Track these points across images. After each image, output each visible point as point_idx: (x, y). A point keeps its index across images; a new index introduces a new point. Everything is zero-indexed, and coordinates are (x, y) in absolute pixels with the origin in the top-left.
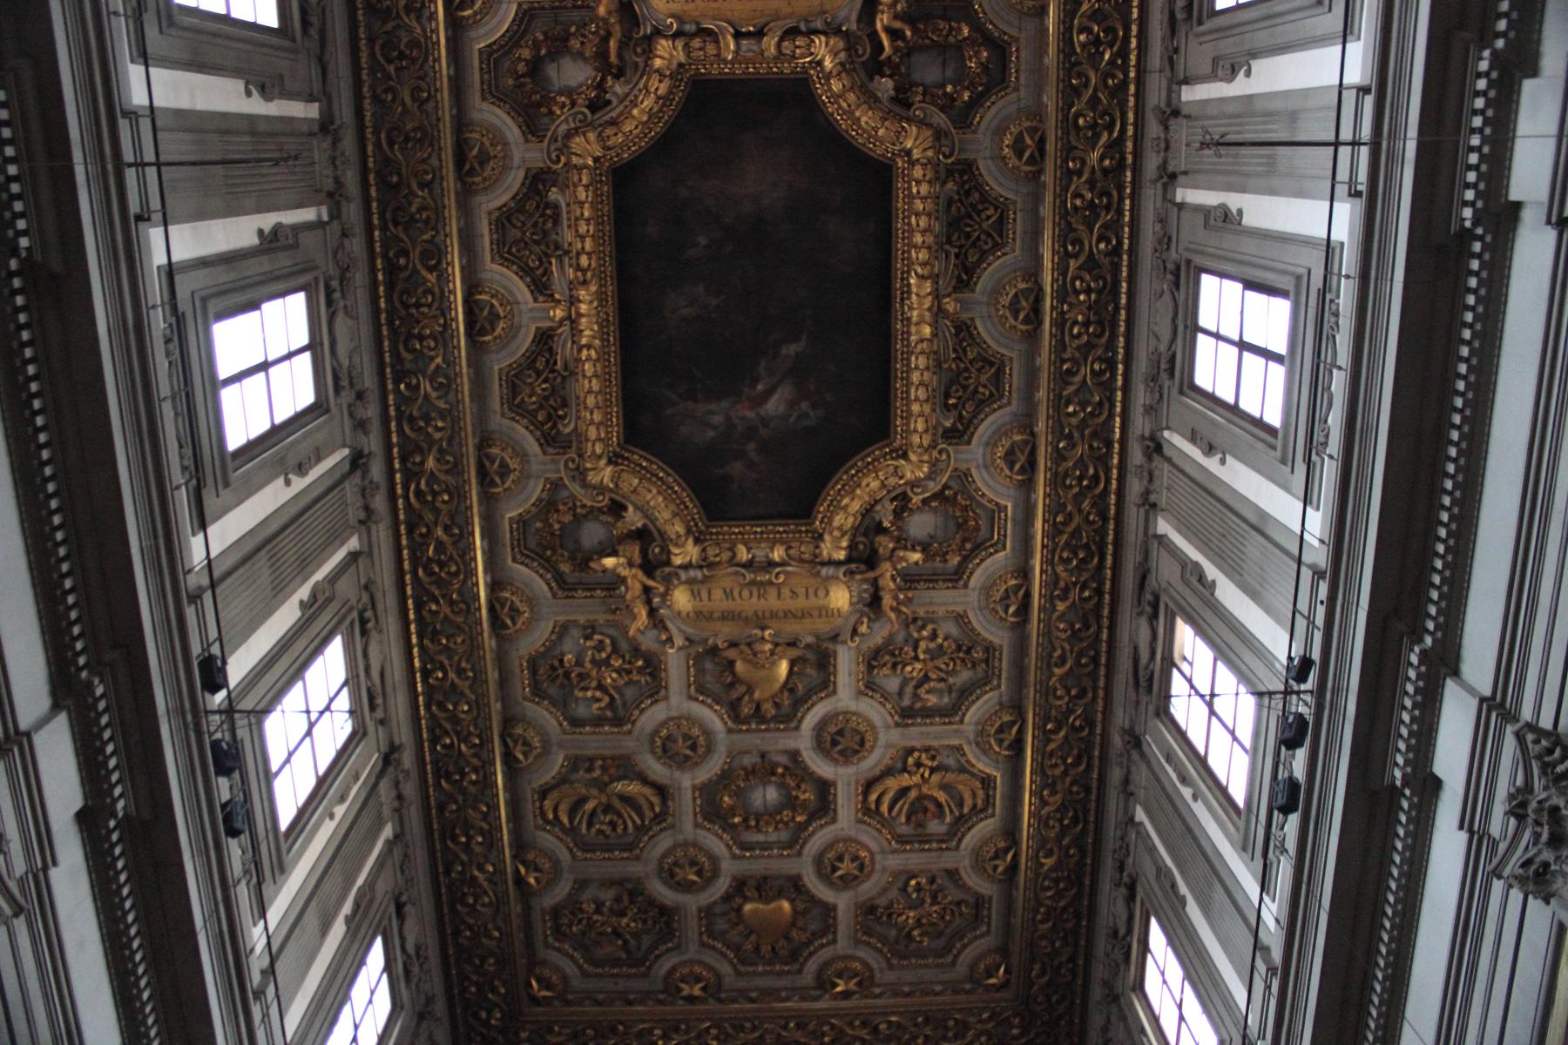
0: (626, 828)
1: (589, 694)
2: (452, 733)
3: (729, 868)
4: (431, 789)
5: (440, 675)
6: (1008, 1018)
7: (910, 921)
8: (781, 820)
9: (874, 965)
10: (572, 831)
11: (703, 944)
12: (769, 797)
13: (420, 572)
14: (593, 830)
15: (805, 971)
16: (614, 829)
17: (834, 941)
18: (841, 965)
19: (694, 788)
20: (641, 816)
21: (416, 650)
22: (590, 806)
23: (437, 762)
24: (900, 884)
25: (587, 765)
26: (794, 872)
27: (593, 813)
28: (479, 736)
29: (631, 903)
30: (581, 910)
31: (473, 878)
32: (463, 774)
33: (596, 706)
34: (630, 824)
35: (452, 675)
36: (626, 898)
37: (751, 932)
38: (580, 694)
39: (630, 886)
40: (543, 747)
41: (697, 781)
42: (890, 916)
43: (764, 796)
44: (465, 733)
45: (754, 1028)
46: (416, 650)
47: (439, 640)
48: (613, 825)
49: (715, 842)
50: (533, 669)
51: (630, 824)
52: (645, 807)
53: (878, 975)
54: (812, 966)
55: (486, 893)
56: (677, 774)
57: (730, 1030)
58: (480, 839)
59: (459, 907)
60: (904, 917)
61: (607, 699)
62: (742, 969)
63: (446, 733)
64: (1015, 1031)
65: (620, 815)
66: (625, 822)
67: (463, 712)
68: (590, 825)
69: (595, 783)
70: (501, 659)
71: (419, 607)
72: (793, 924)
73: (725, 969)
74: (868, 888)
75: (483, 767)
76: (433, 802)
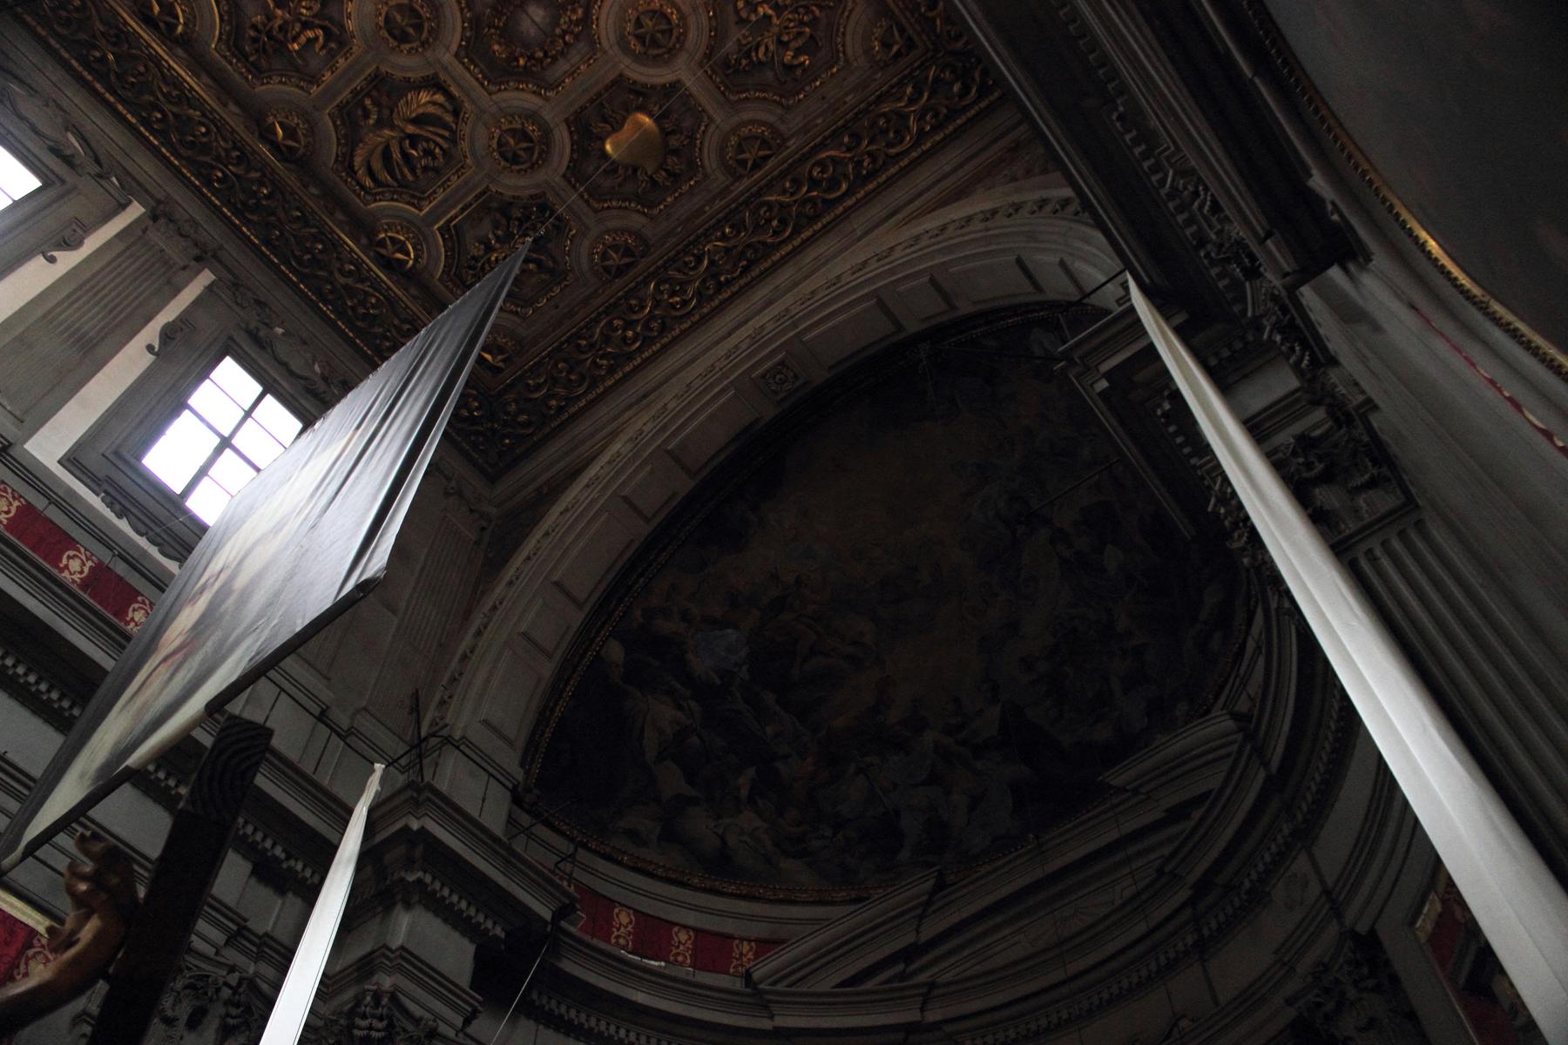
0: (441, 148)
1: (303, 39)
2: (214, 163)
3: (553, 112)
4: (244, 229)
5: (159, 116)
6: (936, 80)
7: (772, 47)
8: (565, 32)
9: (771, 119)
10: (403, 184)
11: (596, 211)
12: (537, 19)
13: (59, 29)
14: (419, 172)
15: (709, 170)
16: (434, 158)
17: (711, 119)
18: (734, 140)
19: (456, 55)
20: (446, 126)
21: (120, 107)
22: (396, 155)
23: (229, 201)
24: (733, 18)
25: (360, 112)
26: (612, 76)
27: (405, 155)
28: (235, 148)
29: (509, 219)
30: (473, 258)
31: (346, 287)
32: (254, 194)
33: (317, 47)
34: (439, 140)
35: (167, 107)
36: (498, 216)
37: (635, 171)
38: (296, 47)
39: (494, 205)
40: (308, 121)
41: (454, 47)
42: (748, 55)
43: (533, 21)
44: (223, 154)
45: (699, 260)
46: (120, 107)
47: (127, 83)
48: (428, 153)
49: (520, 98)
50: (243, 57)
51: (439, 140)
52: (439, 112)
53: (782, 128)
54: (710, 161)
55: (366, 293)
56: (429, 54)
57: (679, 276)
58: (320, 247)
59: (359, 324)
60: (762, 49)
61: (320, 32)
62: (656, 211)
63: (213, 167)
64: (956, 88)
65: (428, 140)
66: (437, 144)
67: (203, 135)
68: (413, 170)
69: (380, 124)
70: (199, 63)
71: (86, 65)
72: (666, 134)
73: (637, 221)
74: (697, 36)
75: (264, 175)
76: (257, 242)
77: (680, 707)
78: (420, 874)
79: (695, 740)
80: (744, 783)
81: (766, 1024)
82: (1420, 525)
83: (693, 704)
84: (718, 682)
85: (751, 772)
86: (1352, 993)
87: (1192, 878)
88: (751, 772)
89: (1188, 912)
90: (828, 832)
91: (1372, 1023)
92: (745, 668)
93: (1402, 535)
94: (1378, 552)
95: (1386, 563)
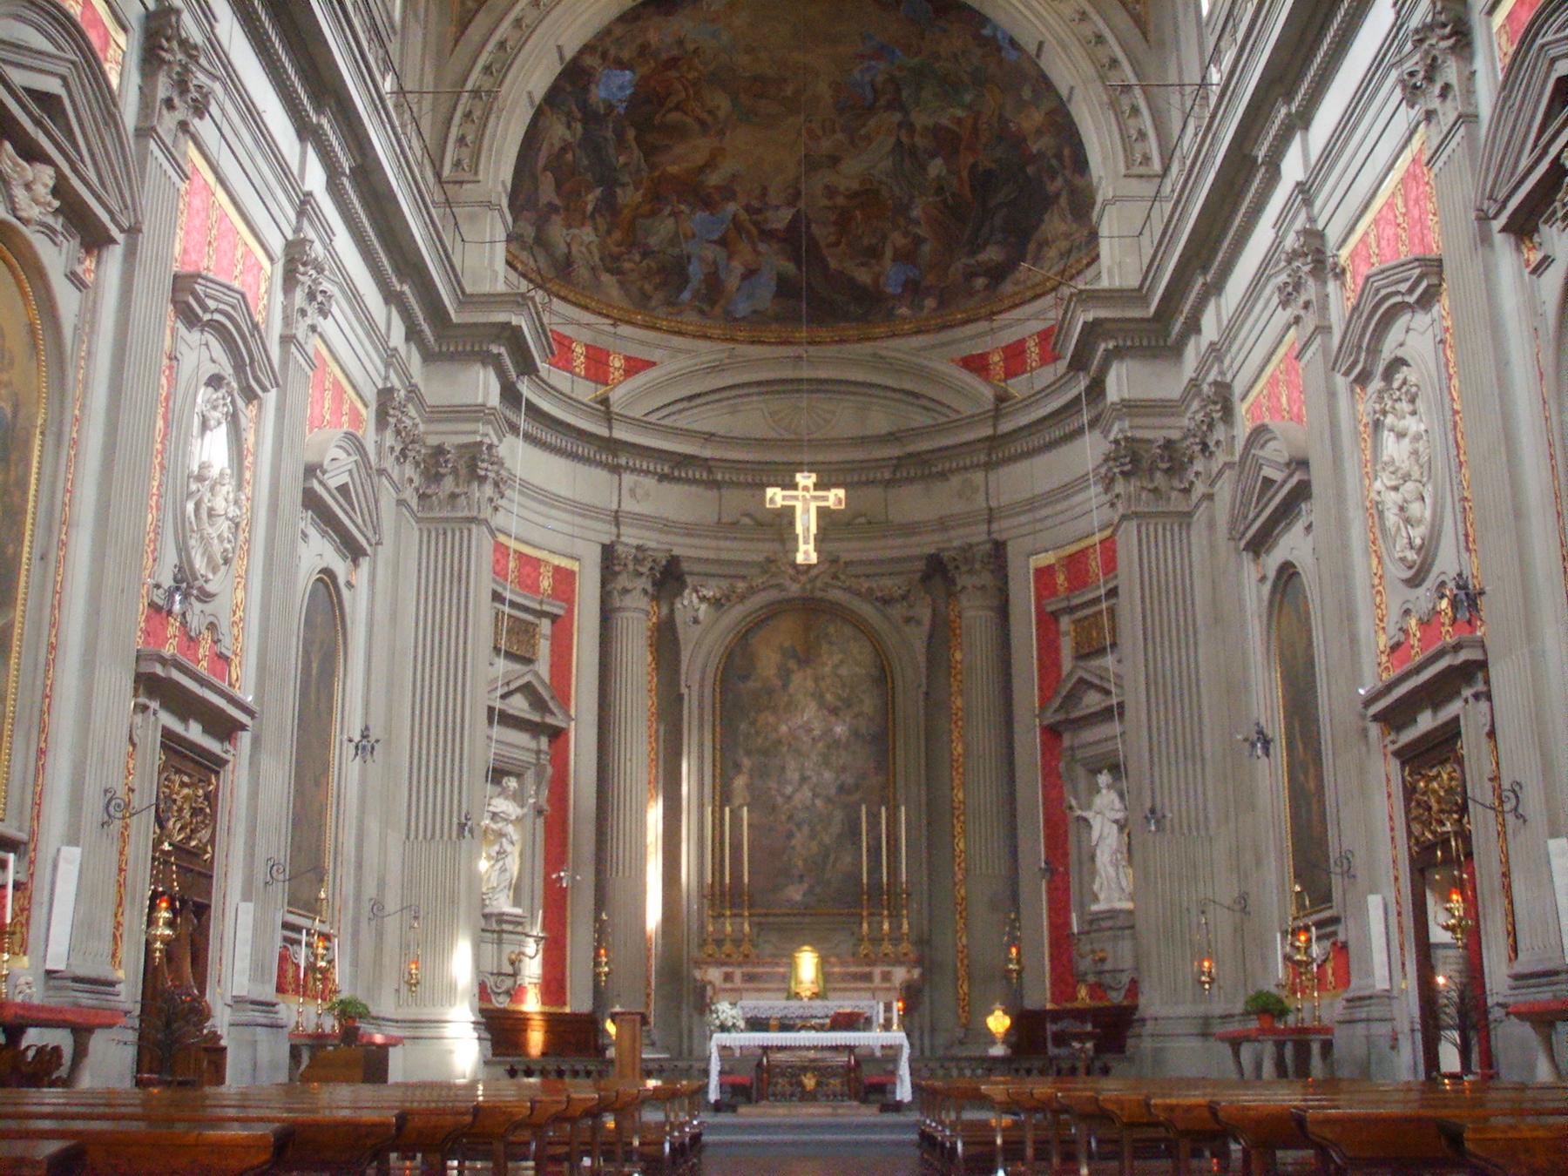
77: (569, 127)
78: (503, 350)
79: (569, 157)
80: (591, 199)
81: (604, 432)
82: (1189, 525)
83: (579, 127)
84: (602, 111)
85: (598, 191)
86: (978, 566)
87: (911, 448)
88: (598, 191)
89: (895, 462)
90: (637, 258)
91: (983, 588)
92: (624, 105)
93: (1180, 526)
94: (1168, 527)
95: (1168, 534)
